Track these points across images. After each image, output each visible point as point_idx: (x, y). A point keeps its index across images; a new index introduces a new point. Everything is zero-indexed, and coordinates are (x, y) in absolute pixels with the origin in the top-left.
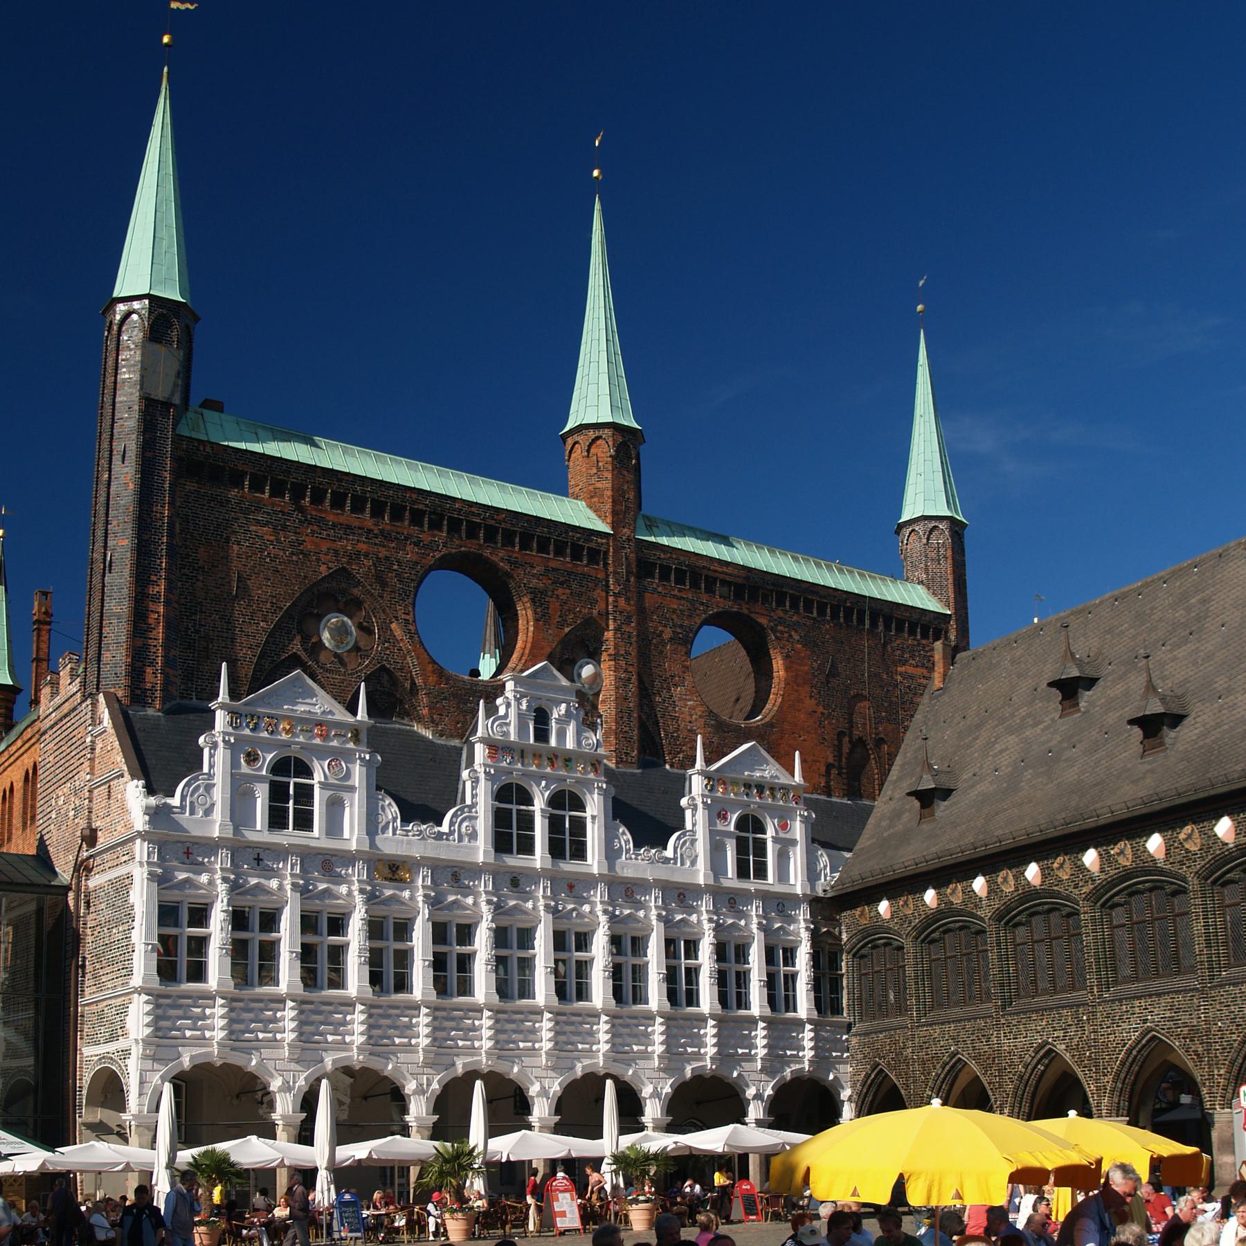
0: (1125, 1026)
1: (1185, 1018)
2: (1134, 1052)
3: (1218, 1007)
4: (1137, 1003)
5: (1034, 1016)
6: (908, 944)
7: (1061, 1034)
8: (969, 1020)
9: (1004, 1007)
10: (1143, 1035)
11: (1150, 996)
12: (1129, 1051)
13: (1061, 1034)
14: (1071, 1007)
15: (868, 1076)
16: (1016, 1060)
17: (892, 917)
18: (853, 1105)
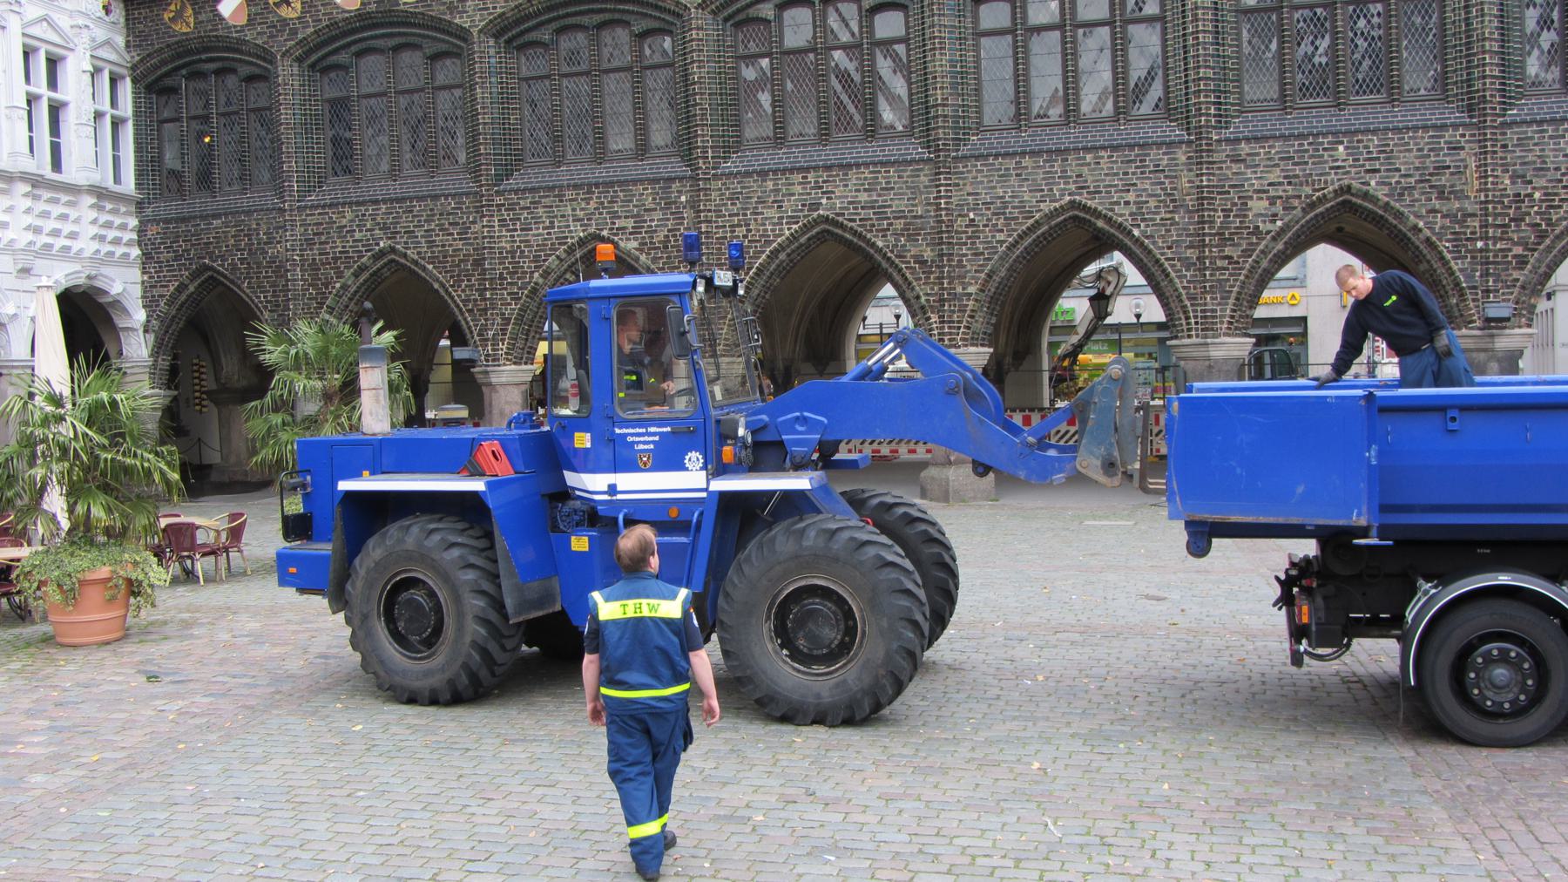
0: (769, 213)
1: (900, 205)
2: (782, 256)
3: (969, 189)
4: (798, 177)
5: (569, 194)
6: (288, 74)
7: (630, 223)
8: (420, 199)
9: (499, 179)
10: (806, 228)
11: (828, 168)
12: (775, 253)
13: (630, 223)
14: (655, 181)
15: (181, 288)
16: (527, 265)
17: (251, 21)
18: (151, 337)
